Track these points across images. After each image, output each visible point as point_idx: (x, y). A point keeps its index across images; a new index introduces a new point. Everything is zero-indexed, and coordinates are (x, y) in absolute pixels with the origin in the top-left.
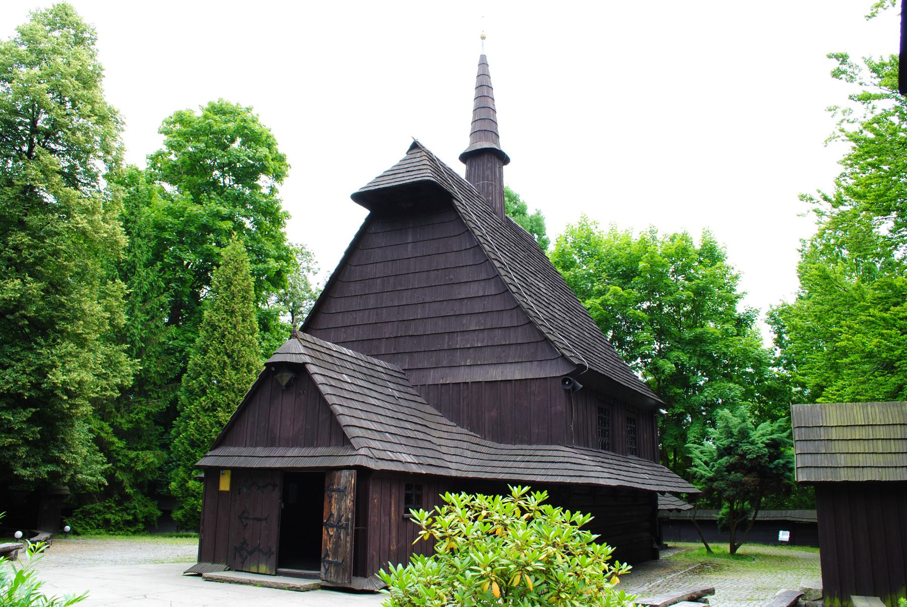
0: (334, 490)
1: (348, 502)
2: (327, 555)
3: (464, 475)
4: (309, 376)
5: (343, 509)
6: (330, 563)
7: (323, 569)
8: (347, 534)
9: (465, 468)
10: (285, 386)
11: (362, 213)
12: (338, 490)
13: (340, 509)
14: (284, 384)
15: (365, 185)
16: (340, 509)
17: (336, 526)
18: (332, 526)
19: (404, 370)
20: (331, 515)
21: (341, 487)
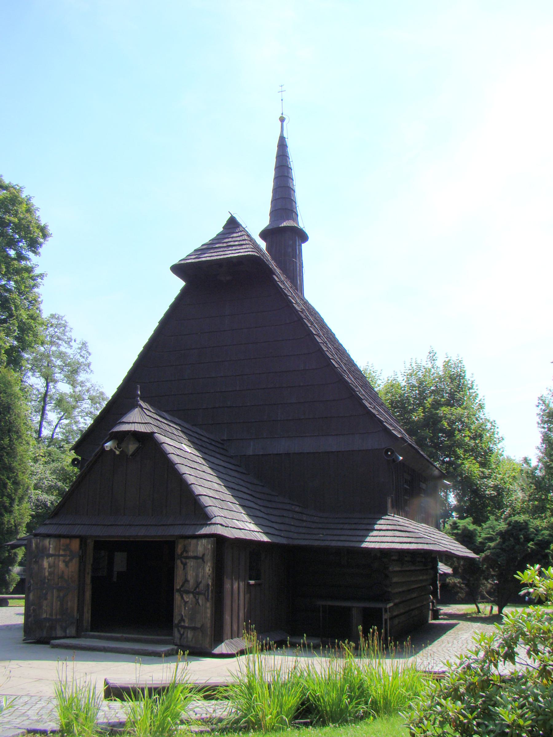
0: (188, 558)
1: (207, 569)
2: (182, 620)
3: (296, 542)
4: (157, 447)
5: (200, 575)
6: (184, 627)
7: (176, 634)
8: (207, 599)
9: (295, 536)
10: (132, 455)
11: (179, 284)
12: (196, 558)
13: (197, 576)
14: (130, 453)
15: (184, 257)
16: (197, 576)
17: (193, 593)
18: (188, 592)
19: (223, 440)
20: (186, 581)
21: (200, 554)
